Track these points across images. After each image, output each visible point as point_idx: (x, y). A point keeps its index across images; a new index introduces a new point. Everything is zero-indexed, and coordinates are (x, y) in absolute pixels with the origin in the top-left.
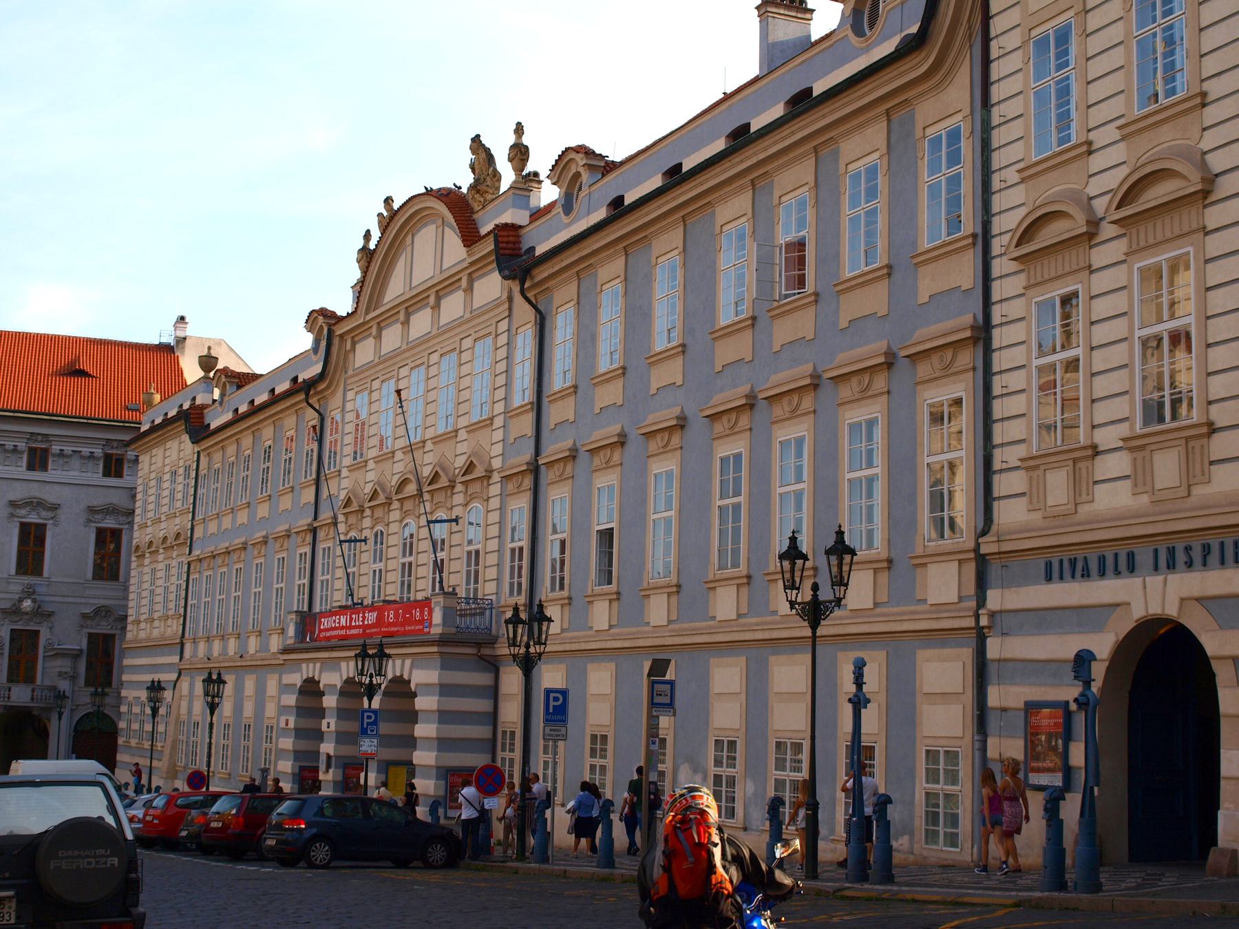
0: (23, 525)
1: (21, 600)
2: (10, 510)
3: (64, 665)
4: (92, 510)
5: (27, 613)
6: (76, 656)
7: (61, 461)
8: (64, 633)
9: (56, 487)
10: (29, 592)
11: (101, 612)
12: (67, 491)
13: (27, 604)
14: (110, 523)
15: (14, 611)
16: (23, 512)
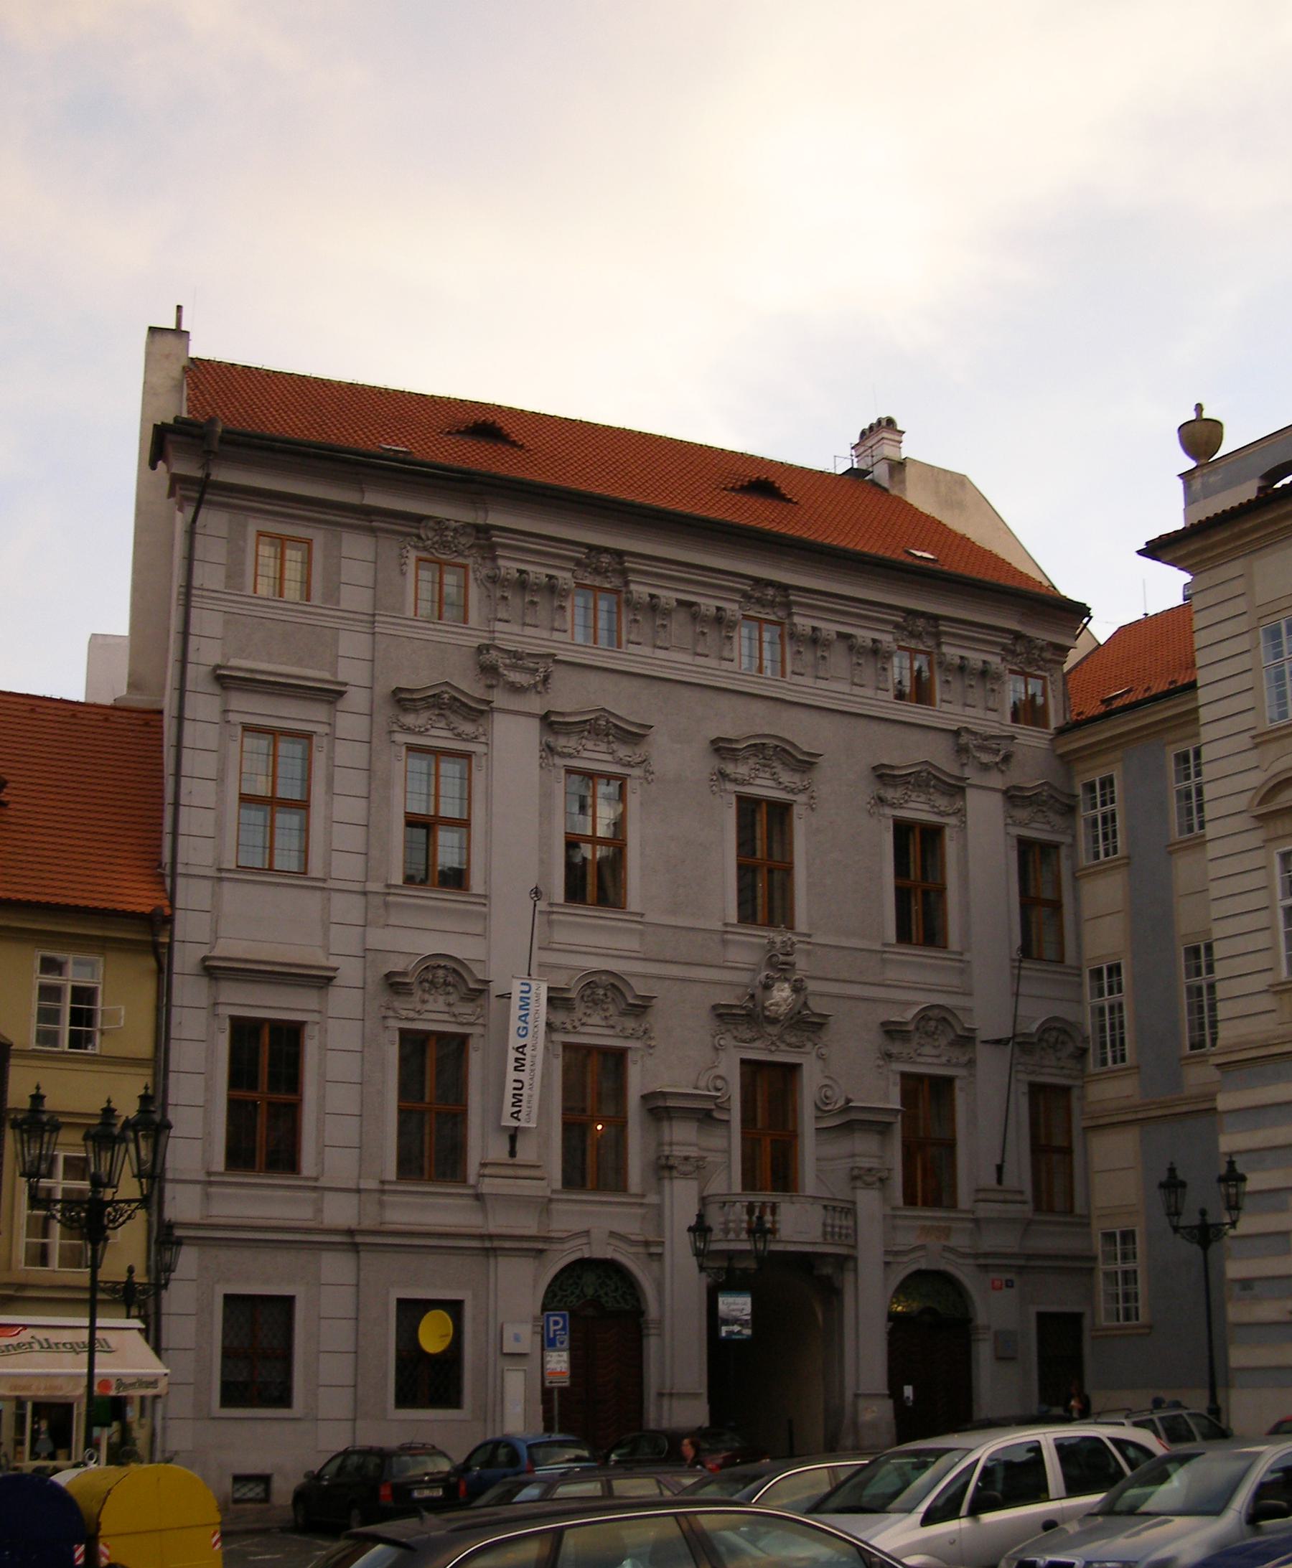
0: (741, 799)
1: (767, 987)
2: (715, 763)
3: (865, 1148)
4: (883, 775)
5: (773, 1021)
6: (876, 1125)
7: (808, 656)
8: (847, 1072)
9: (804, 715)
10: (780, 966)
11: (936, 1021)
12: (826, 725)
13: (782, 994)
14: (918, 810)
15: (740, 1016)
16: (742, 770)
